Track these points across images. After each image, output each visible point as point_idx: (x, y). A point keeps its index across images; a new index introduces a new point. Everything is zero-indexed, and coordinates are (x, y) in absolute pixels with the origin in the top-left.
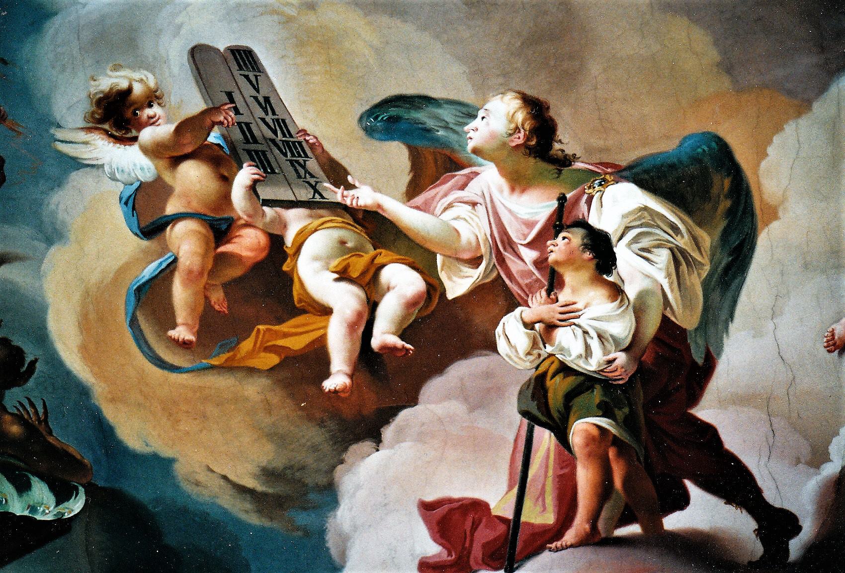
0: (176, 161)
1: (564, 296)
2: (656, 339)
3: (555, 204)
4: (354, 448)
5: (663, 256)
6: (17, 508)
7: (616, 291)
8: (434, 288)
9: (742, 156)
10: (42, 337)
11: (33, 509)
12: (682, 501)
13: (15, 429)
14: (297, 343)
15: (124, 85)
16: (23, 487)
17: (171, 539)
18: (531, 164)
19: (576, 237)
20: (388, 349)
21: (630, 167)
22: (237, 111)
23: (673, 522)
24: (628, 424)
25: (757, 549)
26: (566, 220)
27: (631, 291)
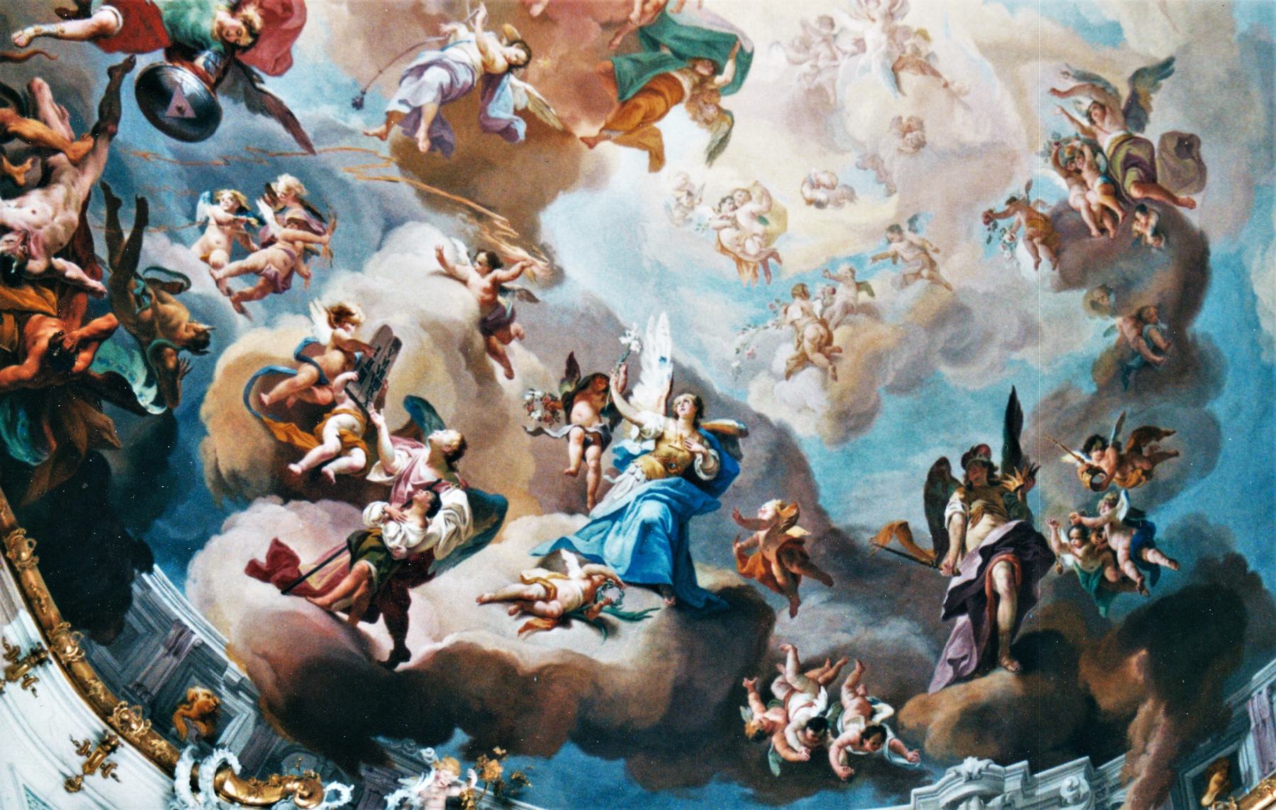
0: (337, 347)
1: (406, 512)
2: (422, 554)
3: (435, 479)
4: (275, 497)
5: (452, 527)
6: (137, 388)
7: (425, 526)
8: (365, 470)
9: (508, 515)
10: (220, 350)
11: (141, 395)
12: (372, 620)
13: (171, 364)
14: (298, 442)
15: (353, 311)
16: (148, 384)
17: (171, 459)
18: (443, 461)
19: (430, 496)
20: (326, 475)
21: (472, 489)
22: (375, 355)
23: (363, 626)
24: (381, 576)
25: (385, 656)
26: (434, 488)
27: (430, 530)
